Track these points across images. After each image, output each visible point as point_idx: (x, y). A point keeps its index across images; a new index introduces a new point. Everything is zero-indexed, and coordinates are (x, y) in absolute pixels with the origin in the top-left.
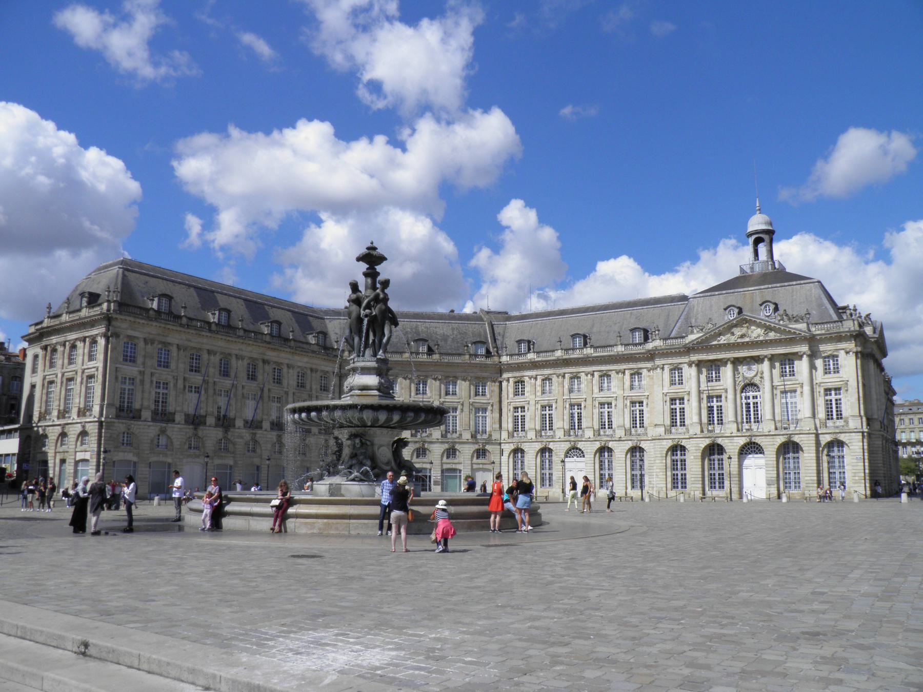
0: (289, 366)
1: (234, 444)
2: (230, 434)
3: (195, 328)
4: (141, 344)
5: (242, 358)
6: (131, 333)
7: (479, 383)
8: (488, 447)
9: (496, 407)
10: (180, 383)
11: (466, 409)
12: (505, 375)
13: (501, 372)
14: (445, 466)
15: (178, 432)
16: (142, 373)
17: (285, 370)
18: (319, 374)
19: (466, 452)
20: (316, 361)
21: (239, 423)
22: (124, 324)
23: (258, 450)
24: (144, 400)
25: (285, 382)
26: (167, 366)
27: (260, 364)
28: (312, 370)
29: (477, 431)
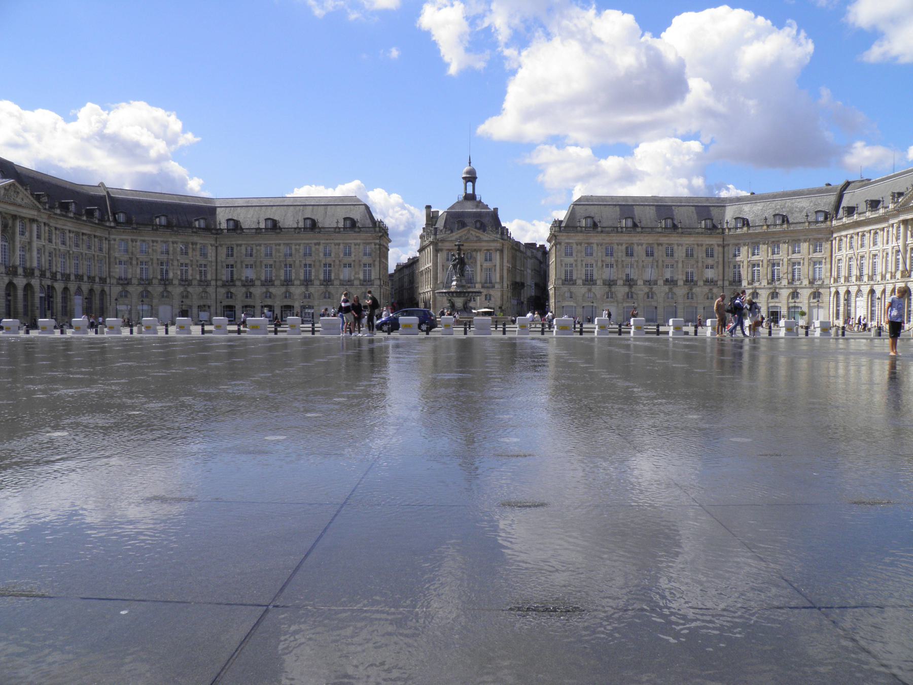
0: (678, 245)
1: (637, 294)
2: (633, 290)
3: (608, 233)
4: (574, 246)
5: (642, 245)
6: (567, 241)
7: (817, 244)
8: (820, 290)
10: (600, 264)
12: (835, 235)
13: (832, 233)
14: (770, 305)
15: (599, 290)
16: (576, 261)
17: (675, 247)
18: (704, 248)
19: (805, 294)
20: (701, 239)
21: (640, 282)
22: (563, 238)
23: (655, 298)
24: (579, 274)
25: (676, 255)
26: (591, 254)
27: (656, 246)
28: (698, 245)
29: (814, 279)
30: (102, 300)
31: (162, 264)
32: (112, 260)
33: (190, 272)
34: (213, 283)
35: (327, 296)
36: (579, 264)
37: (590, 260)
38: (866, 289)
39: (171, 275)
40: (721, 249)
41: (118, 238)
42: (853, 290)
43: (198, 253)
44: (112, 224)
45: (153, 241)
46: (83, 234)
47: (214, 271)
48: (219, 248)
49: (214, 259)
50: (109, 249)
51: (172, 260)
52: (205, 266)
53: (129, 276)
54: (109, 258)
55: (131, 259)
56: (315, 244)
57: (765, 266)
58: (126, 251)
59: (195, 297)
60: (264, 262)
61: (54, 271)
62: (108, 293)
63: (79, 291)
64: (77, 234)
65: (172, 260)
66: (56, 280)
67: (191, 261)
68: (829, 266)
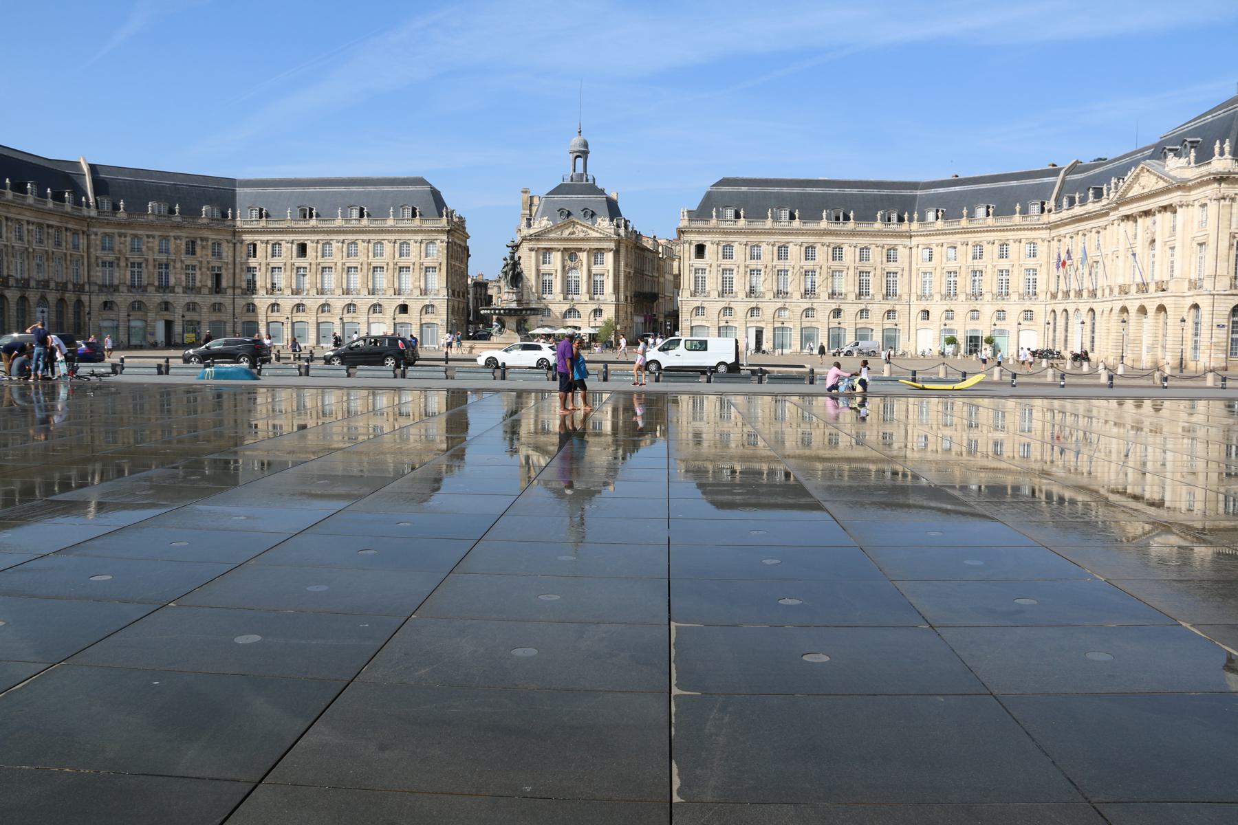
9: (1044, 268)
10: (742, 269)
11: (1016, 272)
30: (78, 314)
31: (160, 266)
32: (93, 260)
33: (198, 277)
34: (230, 291)
35: (376, 308)
36: (714, 269)
37: (727, 263)
38: (1084, 308)
39: (172, 281)
40: (907, 251)
41: (101, 231)
42: (1071, 308)
43: (210, 252)
44: (93, 213)
45: (148, 236)
46: (48, 226)
47: (231, 276)
48: (238, 245)
49: (231, 259)
50: (88, 247)
51: (174, 261)
52: (219, 268)
53: (116, 282)
54: (88, 258)
55: (118, 259)
56: (363, 241)
57: (963, 274)
58: (111, 249)
59: (205, 310)
60: (297, 265)
61: (5, 274)
62: (87, 304)
63: (43, 301)
64: (40, 225)
65: (174, 261)
66: (8, 287)
67: (201, 262)
68: (1045, 276)
